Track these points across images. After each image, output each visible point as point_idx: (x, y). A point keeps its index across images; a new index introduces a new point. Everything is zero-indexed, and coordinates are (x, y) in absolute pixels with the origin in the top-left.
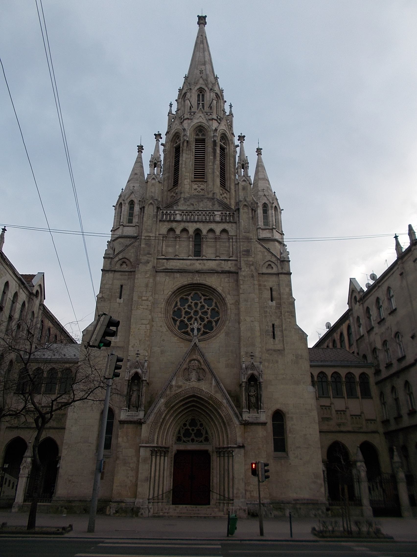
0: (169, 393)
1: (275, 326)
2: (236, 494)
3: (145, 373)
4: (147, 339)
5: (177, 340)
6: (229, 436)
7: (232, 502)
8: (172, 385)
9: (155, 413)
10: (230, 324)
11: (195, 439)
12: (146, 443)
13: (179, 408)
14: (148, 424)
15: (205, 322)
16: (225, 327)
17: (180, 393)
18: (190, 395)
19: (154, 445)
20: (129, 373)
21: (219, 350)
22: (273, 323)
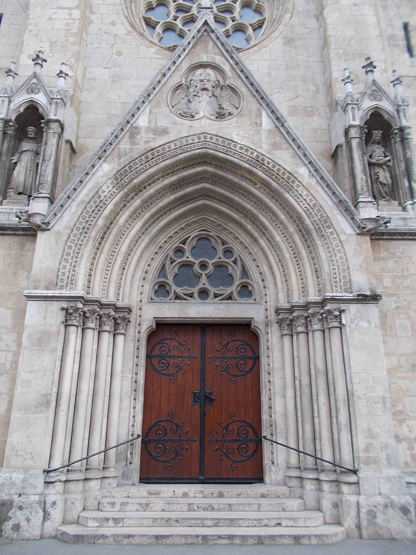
0: (128, 146)
1: (410, 28)
2: (367, 449)
3: (57, 103)
4: (72, 39)
5: (155, 53)
6: (326, 268)
7: (353, 478)
8: (136, 128)
9: (82, 202)
10: (295, 20)
11: (212, 290)
12: (47, 288)
13: (160, 194)
14: (58, 232)
15: (229, 27)
16: (281, 27)
17: (164, 149)
18: (193, 153)
19: (74, 293)
20: (10, 102)
21: (270, 75)
22: (406, 21)
